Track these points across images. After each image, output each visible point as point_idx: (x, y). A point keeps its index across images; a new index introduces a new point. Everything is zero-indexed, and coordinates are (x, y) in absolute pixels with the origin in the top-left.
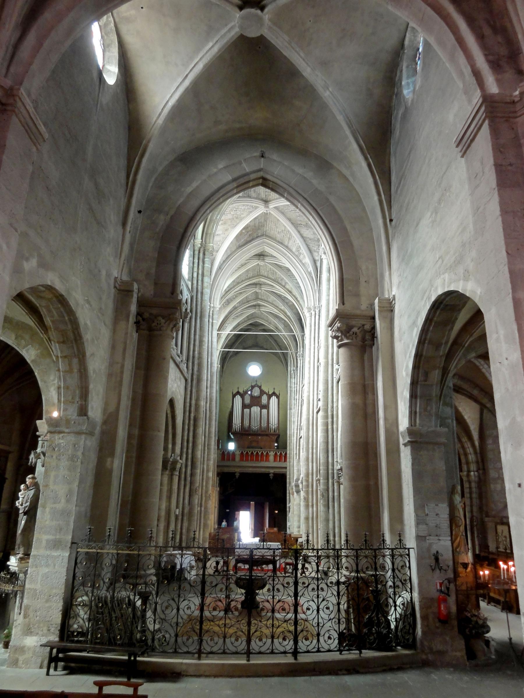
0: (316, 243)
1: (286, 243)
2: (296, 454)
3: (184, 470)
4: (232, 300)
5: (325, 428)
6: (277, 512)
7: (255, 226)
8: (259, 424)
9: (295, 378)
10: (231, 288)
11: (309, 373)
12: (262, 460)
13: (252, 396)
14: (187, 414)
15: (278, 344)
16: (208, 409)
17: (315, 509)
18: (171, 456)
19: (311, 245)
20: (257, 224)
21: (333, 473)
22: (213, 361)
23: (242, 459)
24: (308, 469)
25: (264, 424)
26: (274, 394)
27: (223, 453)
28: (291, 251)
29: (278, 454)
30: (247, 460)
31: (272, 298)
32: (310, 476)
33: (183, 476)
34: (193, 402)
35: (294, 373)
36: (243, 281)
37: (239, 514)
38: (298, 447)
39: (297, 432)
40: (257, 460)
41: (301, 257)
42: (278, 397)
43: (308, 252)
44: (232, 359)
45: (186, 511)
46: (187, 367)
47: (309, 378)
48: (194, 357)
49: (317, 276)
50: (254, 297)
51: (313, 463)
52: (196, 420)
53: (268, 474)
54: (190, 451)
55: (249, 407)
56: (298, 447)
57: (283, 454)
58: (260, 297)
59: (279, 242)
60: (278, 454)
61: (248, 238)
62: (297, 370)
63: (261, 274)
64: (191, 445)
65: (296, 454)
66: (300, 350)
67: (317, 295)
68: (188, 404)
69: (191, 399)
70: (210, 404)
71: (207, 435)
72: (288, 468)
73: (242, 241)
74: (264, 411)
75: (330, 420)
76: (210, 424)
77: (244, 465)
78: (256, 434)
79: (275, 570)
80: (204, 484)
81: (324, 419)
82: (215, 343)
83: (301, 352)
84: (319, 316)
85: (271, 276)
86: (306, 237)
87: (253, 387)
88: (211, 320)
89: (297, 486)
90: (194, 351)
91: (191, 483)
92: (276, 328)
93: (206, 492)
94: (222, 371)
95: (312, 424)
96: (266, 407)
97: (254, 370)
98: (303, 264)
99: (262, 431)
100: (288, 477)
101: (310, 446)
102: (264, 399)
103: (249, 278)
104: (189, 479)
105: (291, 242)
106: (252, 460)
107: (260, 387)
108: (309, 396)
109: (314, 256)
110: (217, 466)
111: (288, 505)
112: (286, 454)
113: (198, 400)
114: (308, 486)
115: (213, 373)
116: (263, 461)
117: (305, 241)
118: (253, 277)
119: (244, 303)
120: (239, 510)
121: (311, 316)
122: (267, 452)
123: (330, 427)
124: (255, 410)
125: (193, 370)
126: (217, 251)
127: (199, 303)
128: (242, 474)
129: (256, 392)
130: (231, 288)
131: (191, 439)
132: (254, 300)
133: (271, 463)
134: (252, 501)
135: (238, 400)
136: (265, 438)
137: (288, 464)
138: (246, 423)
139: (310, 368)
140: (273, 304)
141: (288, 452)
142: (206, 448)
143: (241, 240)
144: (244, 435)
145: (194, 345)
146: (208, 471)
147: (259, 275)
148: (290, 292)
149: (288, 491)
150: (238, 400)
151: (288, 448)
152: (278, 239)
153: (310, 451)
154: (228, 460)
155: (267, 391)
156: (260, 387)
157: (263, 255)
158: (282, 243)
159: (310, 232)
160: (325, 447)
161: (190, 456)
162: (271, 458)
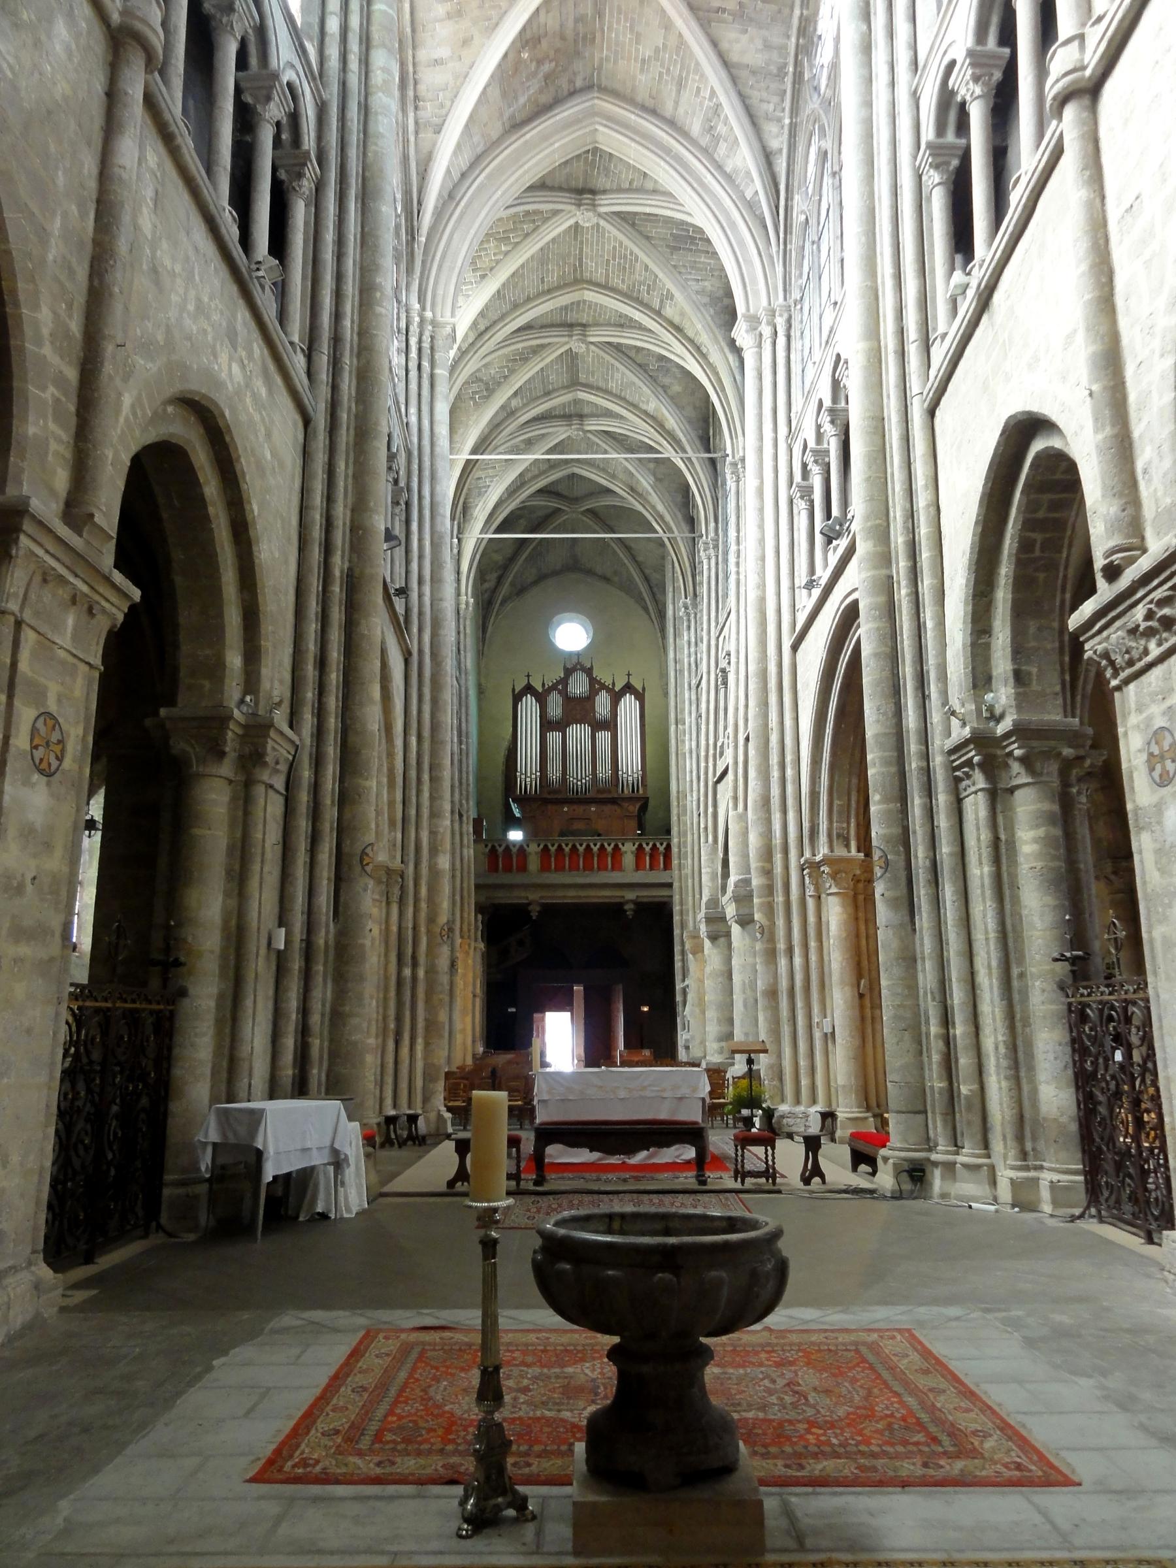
0: (774, 86)
1: (668, 109)
2: (706, 828)
3: (306, 774)
4: (499, 384)
5: (882, 599)
6: (646, 1009)
7: (563, 38)
9: (689, 627)
10: (495, 322)
11: (761, 527)
12: (602, 867)
13: (568, 700)
14: (316, 554)
15: (634, 558)
16: (427, 650)
17: (798, 960)
18: (242, 701)
19: (755, 95)
20: (570, 24)
21: (927, 772)
22: (438, 498)
23: (545, 868)
24: (768, 834)
25: (604, 771)
27: (493, 850)
28: (686, 134)
29: (647, 849)
30: (560, 868)
31: (623, 376)
32: (778, 858)
33: (304, 797)
34: (341, 512)
35: (688, 615)
36: (529, 299)
37: (543, 1019)
38: (710, 810)
39: (707, 768)
40: (588, 867)
41: (722, 150)
42: (640, 697)
43: (746, 120)
44: (509, 606)
45: (325, 936)
46: (310, 374)
47: (762, 541)
48: (336, 340)
49: (777, 207)
50: (565, 379)
51: (784, 812)
52: (353, 584)
53: (615, 910)
54: (333, 703)
55: (560, 726)
56: (710, 810)
57: (662, 849)
58: (582, 377)
59: (644, 108)
60: (647, 849)
61: (541, 91)
62: (695, 605)
63: (586, 275)
64: (334, 677)
65: (706, 828)
66: (706, 528)
67: (779, 269)
68: (317, 517)
69: (329, 499)
70: (434, 635)
71: (426, 733)
72: (676, 885)
73: (522, 100)
74: (604, 737)
75: (902, 564)
76: (435, 701)
77: (548, 881)
78: (581, 800)
79: (701, 1163)
80: (424, 891)
81: (875, 568)
82: (443, 442)
83: (712, 534)
84: (788, 337)
85: (616, 282)
86: (739, 66)
87: (569, 672)
88: (426, 364)
89: (716, 920)
90: (337, 316)
91: (343, 830)
92: (632, 489)
93: (431, 920)
95: (774, 686)
96: (610, 725)
97: (571, 636)
98: (729, 178)
99: (599, 791)
100: (676, 909)
101: (774, 759)
102: (602, 704)
103: (549, 291)
104: (330, 814)
105: (686, 95)
106: (574, 867)
107: (589, 672)
108: (762, 600)
109: (766, 136)
110: (477, 887)
111: (679, 986)
112: (668, 848)
113: (360, 506)
114: (770, 889)
115: (441, 537)
116: (606, 869)
117: (734, 80)
118: (558, 288)
119: (538, 398)
120: (542, 1009)
121: (760, 346)
122: (616, 846)
123: (903, 593)
124: (578, 733)
125: (335, 388)
126: (438, 130)
127: (354, 138)
128: (549, 910)
129: (579, 686)
130: (495, 322)
131: (335, 655)
132: (564, 387)
133: (629, 872)
134: (578, 983)
135: (529, 709)
136: (607, 809)
137: (676, 872)
138: (554, 773)
139: (761, 510)
140: (624, 399)
141: (675, 841)
142: (426, 777)
143: (516, 98)
144: (548, 803)
145: (338, 295)
146: (434, 851)
147: (579, 281)
148: (678, 329)
149: (677, 948)
150: (529, 709)
151: (674, 830)
152: (642, 96)
153: (775, 774)
154: (508, 869)
155: (608, 682)
156: (589, 672)
157: (593, 192)
158: (654, 112)
159: (751, 40)
160: (887, 673)
161: (332, 723)
162: (629, 860)
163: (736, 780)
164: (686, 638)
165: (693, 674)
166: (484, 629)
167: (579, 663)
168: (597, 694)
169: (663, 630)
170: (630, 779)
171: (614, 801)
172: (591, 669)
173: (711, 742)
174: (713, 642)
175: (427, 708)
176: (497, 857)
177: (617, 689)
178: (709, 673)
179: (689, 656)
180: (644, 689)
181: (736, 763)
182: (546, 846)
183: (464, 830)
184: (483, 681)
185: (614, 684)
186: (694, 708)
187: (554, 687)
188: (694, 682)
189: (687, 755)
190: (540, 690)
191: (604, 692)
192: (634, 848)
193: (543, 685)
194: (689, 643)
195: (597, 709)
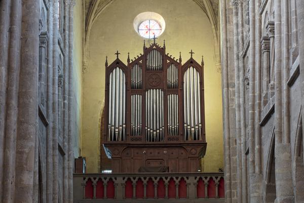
8: (162, 123)
9: (237, 14)
13: (147, 70)
26: (191, 63)
39: (253, 114)
56: (257, 147)
57: (217, 181)
65: (253, 162)
71: (16, 64)
74: (173, 99)
94: (86, 31)
97: (151, 26)
99: (169, 139)
102: (172, 75)
112: (222, 180)
122: (182, 179)
124: (154, 96)
129: (155, 62)
136: (176, 151)
138: (136, 125)
142: (14, 102)
155: (177, 58)
163: (281, 118)
164: (235, 22)
165: (241, 48)
166: (87, 24)
167: (155, 44)
168: (168, 67)
169: (216, 24)
170: (193, 129)
171: (180, 146)
172: (164, 49)
173: (257, 94)
174: (257, 18)
175: (17, 43)
176: (93, 187)
177: (183, 63)
178: (254, 41)
179: (238, 34)
180: (203, 63)
181: (280, 104)
182: (129, 179)
183: (66, 165)
184: (85, 60)
185: (180, 60)
186: (241, 73)
187: (136, 62)
188: (241, 54)
189: (237, 109)
190: (126, 64)
191: (173, 66)
192: (196, 181)
193: (128, 60)
194: (237, 25)
195: (169, 78)
